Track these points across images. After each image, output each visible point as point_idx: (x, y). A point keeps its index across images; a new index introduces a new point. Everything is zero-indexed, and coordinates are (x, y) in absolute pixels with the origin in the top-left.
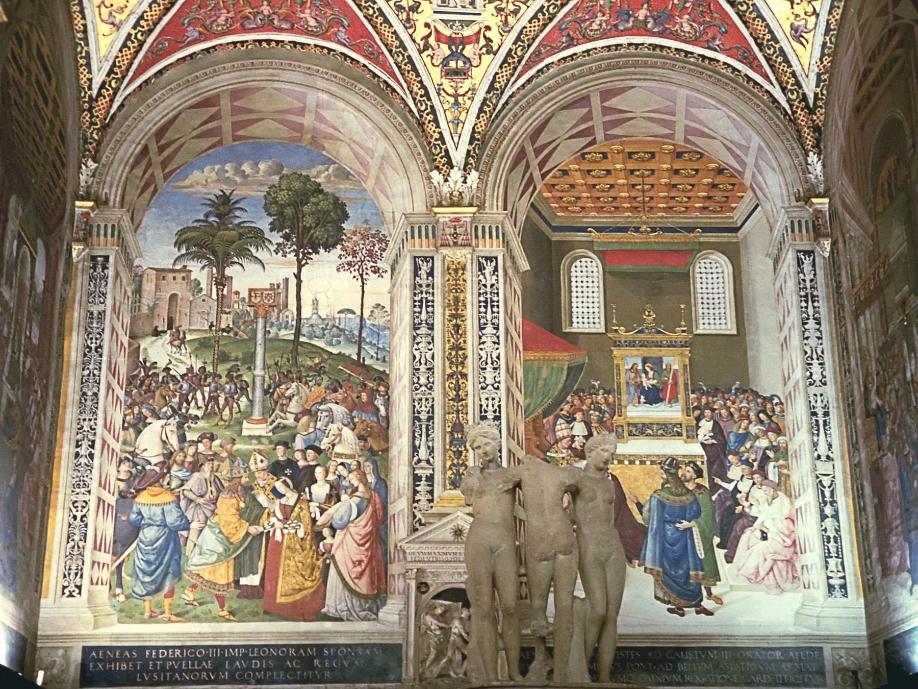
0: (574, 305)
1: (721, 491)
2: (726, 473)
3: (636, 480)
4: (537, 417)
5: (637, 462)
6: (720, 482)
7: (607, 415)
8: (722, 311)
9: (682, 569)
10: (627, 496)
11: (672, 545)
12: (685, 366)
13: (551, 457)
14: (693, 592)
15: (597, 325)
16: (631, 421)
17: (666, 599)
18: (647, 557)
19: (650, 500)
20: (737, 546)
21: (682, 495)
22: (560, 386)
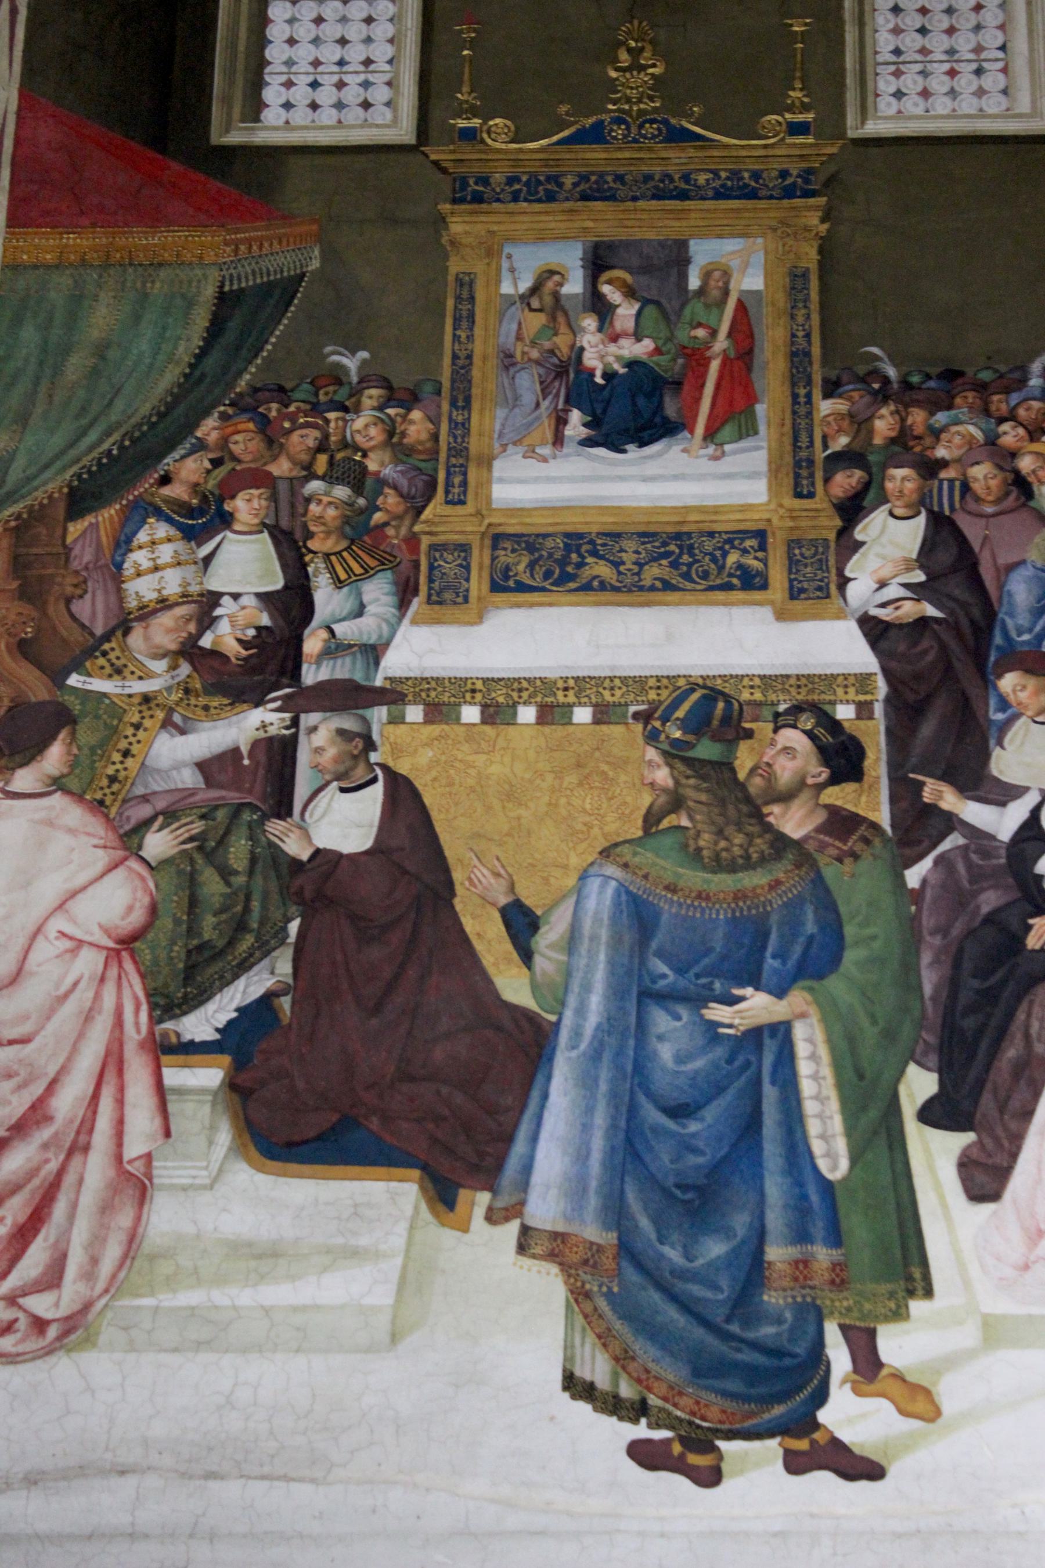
0: (277, 32)
1: (953, 841)
2: (985, 756)
3: (511, 795)
4: (38, 515)
5: (527, 714)
6: (949, 800)
7: (390, 500)
8: (992, 38)
9: (728, 1232)
10: (458, 876)
11: (679, 1112)
12: (797, 279)
13: (86, 695)
14: (777, 1353)
15: (381, 115)
16: (513, 527)
17: (627, 1390)
18: (538, 1178)
19: (579, 892)
20: (1028, 1114)
21: (748, 864)
22: (170, 377)
